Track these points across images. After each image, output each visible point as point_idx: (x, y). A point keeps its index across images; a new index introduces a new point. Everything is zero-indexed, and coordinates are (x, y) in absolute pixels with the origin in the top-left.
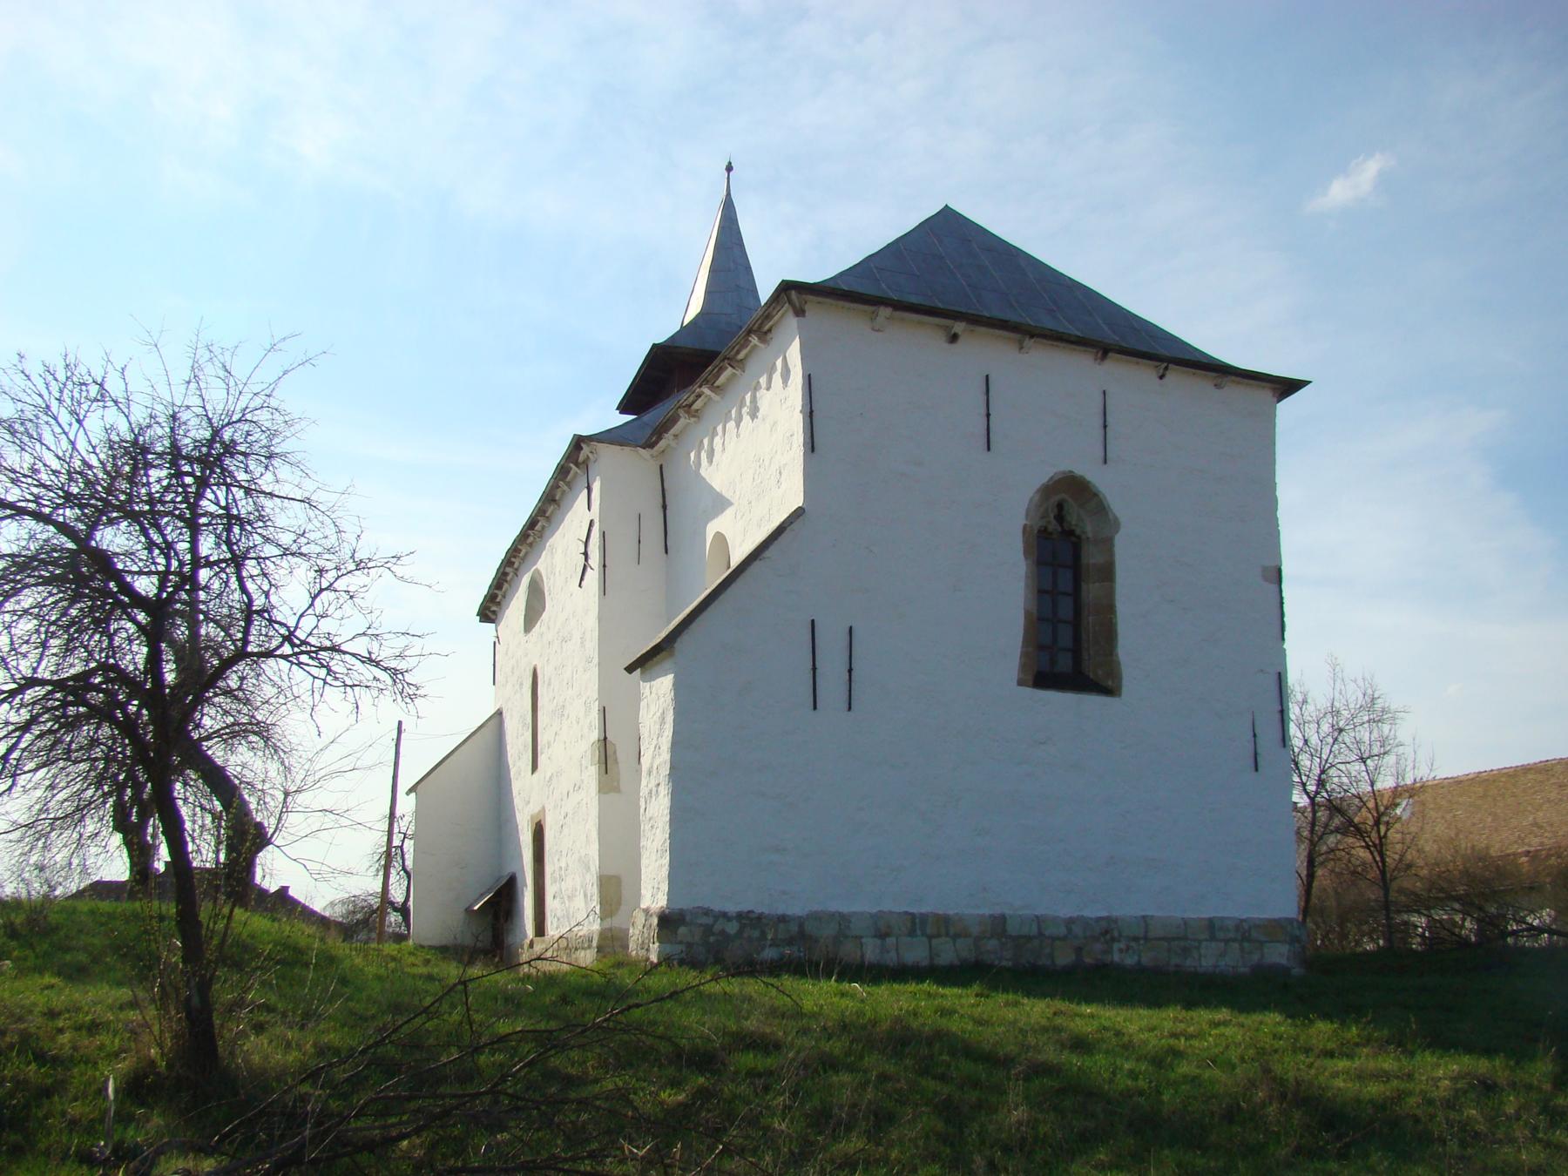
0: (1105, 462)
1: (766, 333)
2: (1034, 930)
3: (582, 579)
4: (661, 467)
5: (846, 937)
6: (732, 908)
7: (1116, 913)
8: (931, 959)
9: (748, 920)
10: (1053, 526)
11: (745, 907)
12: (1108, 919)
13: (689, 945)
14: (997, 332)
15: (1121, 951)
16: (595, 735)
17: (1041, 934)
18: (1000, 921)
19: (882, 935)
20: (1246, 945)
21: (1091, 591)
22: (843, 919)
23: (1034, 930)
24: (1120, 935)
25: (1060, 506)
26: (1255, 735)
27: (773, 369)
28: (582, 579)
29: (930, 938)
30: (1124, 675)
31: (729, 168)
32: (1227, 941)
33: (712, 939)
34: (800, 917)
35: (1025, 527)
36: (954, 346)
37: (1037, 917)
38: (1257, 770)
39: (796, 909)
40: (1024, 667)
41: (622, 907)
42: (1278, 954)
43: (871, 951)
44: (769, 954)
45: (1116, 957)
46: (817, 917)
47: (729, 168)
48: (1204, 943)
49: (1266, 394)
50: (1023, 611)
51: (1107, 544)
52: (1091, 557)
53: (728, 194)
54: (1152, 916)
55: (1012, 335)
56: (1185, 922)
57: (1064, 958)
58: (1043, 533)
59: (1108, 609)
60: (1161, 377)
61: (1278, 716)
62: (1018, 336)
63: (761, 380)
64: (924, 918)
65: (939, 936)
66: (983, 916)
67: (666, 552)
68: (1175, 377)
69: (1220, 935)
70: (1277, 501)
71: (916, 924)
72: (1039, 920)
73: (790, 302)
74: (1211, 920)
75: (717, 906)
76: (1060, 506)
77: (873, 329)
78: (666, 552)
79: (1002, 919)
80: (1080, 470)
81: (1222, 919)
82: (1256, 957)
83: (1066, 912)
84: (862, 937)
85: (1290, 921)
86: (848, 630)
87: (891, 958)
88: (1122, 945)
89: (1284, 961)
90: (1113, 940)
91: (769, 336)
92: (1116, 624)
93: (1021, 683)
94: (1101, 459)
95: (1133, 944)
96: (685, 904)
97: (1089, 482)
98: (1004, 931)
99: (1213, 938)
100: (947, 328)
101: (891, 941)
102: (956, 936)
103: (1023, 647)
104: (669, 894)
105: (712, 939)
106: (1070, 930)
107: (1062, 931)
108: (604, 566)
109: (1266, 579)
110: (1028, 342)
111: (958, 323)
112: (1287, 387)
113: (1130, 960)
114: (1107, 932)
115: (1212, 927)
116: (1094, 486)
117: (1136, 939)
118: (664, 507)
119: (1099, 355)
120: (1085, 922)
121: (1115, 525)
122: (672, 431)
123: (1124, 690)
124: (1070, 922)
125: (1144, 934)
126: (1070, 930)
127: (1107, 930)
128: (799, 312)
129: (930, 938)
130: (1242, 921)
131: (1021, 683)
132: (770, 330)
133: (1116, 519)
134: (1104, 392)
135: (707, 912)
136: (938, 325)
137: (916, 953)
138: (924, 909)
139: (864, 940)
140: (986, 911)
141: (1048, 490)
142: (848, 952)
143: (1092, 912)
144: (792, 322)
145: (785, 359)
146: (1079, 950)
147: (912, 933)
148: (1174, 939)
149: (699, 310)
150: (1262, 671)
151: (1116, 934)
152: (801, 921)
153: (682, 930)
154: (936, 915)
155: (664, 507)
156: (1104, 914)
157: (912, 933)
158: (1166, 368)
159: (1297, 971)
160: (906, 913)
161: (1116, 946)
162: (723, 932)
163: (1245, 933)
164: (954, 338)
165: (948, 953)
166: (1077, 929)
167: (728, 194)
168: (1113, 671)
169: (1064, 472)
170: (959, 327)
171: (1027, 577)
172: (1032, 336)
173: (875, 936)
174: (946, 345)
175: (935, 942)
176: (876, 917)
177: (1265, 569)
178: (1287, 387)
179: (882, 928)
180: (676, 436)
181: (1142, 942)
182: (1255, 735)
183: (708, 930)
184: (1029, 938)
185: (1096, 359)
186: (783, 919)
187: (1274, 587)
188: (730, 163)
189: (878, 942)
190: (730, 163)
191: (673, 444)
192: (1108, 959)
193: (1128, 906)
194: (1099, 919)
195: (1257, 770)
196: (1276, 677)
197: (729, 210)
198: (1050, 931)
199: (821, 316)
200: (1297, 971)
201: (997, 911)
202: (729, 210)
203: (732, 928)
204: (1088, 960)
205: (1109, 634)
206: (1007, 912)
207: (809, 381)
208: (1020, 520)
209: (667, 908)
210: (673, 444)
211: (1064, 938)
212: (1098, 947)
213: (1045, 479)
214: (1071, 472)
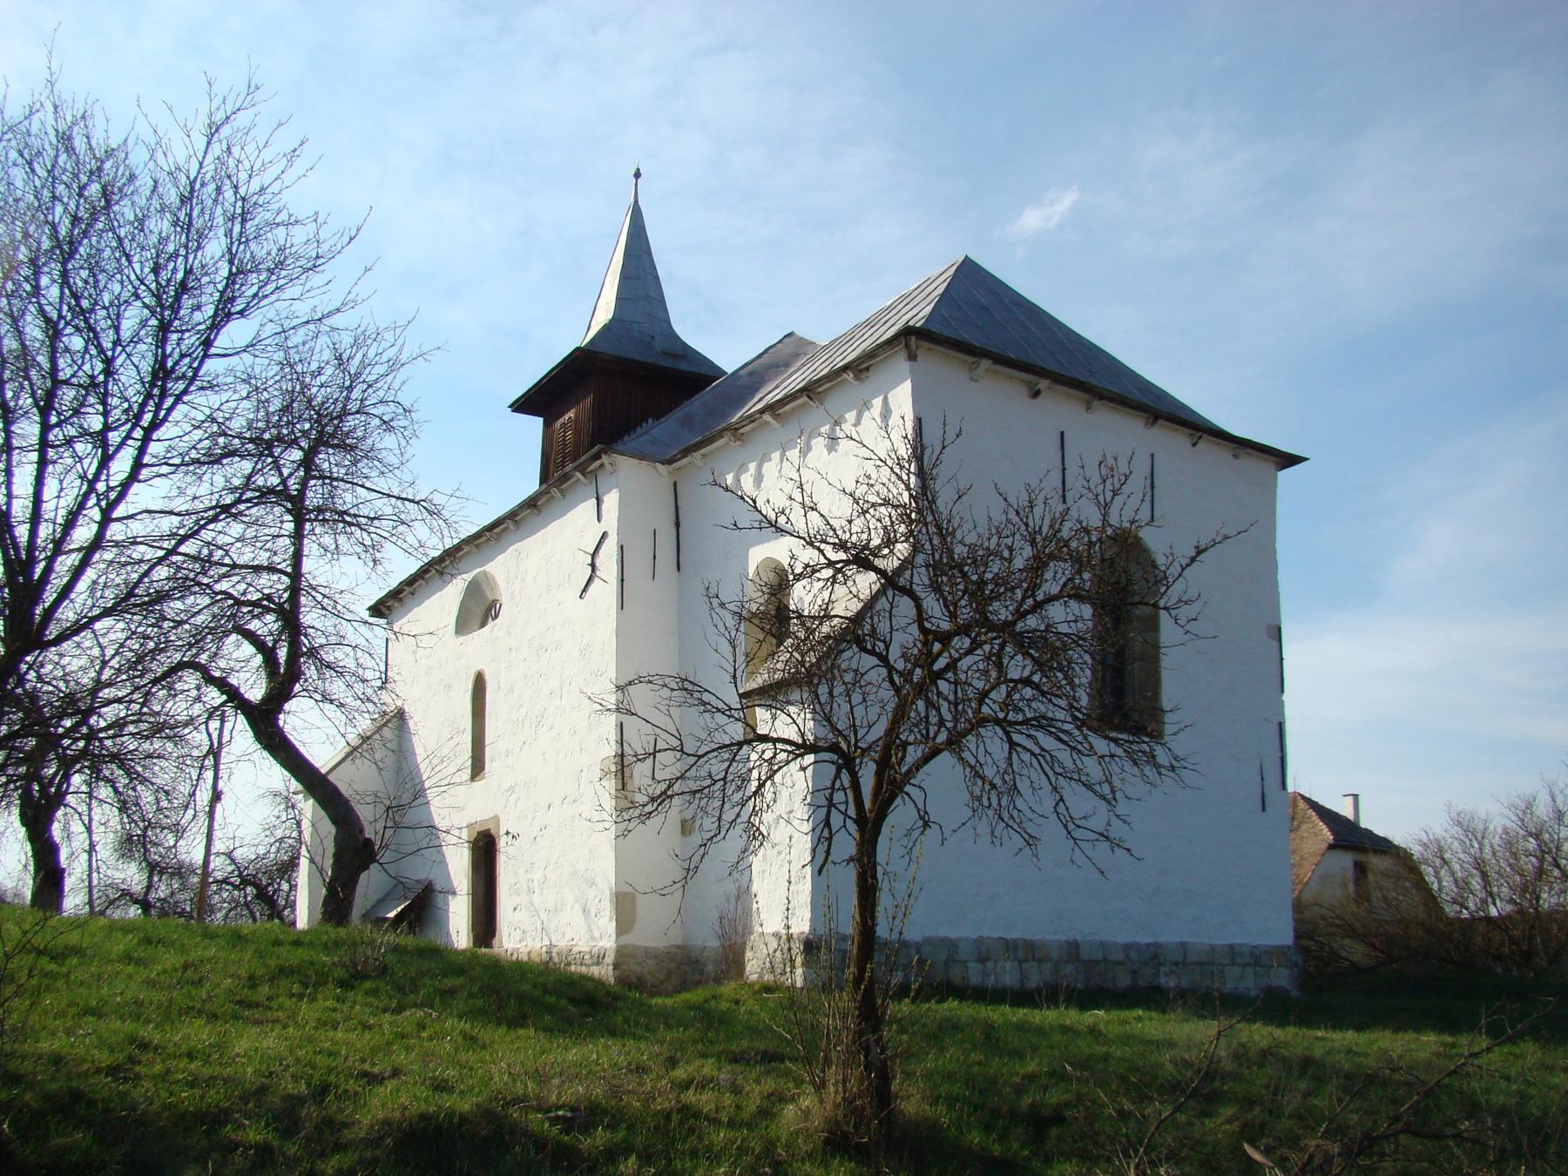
1: (861, 371)
2: (1100, 956)
3: (585, 590)
4: (675, 484)
5: (955, 961)
7: (1159, 940)
8: (1022, 982)
12: (1156, 945)
14: (1071, 391)
16: (611, 750)
17: (1105, 959)
19: (983, 960)
20: (1257, 969)
22: (951, 945)
27: (866, 406)
28: (585, 590)
29: (1021, 962)
31: (638, 175)
32: (1244, 965)
34: (917, 943)
36: (1037, 401)
38: (1264, 810)
41: (637, 925)
42: (1281, 978)
46: (929, 941)
47: (638, 175)
48: (1227, 968)
49: (1266, 466)
53: (636, 201)
55: (1076, 393)
56: (1213, 948)
57: (1124, 981)
60: (1194, 445)
61: (1279, 761)
62: (1086, 396)
63: (847, 416)
64: (1015, 942)
65: (1027, 961)
66: (1059, 941)
67: (679, 569)
69: (1239, 960)
71: (1010, 947)
73: (907, 346)
74: (1231, 947)
77: (971, 379)
78: (679, 569)
81: (1240, 945)
83: (1123, 937)
84: (966, 962)
85: (1289, 947)
89: (1284, 984)
90: (1160, 964)
91: (865, 373)
95: (1174, 967)
96: (821, 931)
98: (1078, 955)
99: (1233, 963)
100: (1029, 384)
101: (990, 964)
102: (1040, 961)
104: (812, 920)
106: (1127, 956)
107: (1121, 956)
108: (622, 580)
110: (1097, 404)
112: (1289, 460)
114: (1155, 956)
117: (1176, 964)
118: (678, 525)
119: (1151, 420)
122: (703, 451)
124: (1127, 947)
125: (1183, 958)
126: (1127, 956)
127: (1154, 955)
128: (912, 357)
130: (1255, 947)
132: (867, 369)
134: (1152, 455)
136: (1023, 381)
139: (968, 965)
142: (956, 975)
143: (1144, 938)
144: (901, 364)
145: (886, 399)
146: (1134, 973)
149: (610, 316)
151: (1162, 959)
154: (1024, 940)
155: (678, 525)
156: (1151, 940)
158: (1200, 437)
159: (1295, 993)
160: (1000, 938)
161: (1163, 969)
163: (1258, 958)
164: (1036, 394)
166: (1133, 955)
167: (636, 201)
170: (1043, 384)
172: (1101, 398)
173: (978, 961)
174: (1028, 400)
175: (1025, 965)
176: (979, 941)
177: (1269, 627)
178: (1289, 460)
180: (704, 456)
184: (1096, 962)
185: (1146, 424)
188: (638, 170)
189: (980, 965)
190: (638, 170)
191: (699, 463)
193: (1169, 934)
194: (1148, 945)
195: (1264, 810)
196: (1277, 727)
198: (1113, 956)
200: (1295, 993)
204: (1141, 983)
206: (1079, 938)
209: (810, 933)
210: (699, 463)
211: (1121, 963)
212: (1148, 971)
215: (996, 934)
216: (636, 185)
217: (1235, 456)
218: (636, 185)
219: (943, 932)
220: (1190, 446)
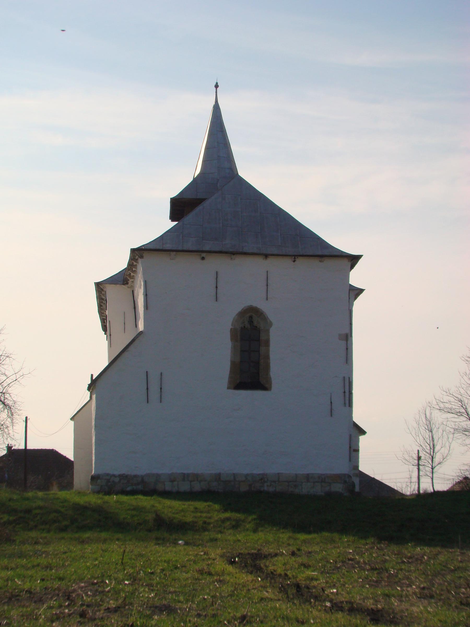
0: (267, 300)
6: (117, 473)
9: (122, 477)
10: (248, 326)
11: (122, 472)
12: (263, 474)
15: (268, 486)
18: (218, 477)
19: (172, 481)
21: (263, 349)
22: (158, 475)
24: (268, 480)
25: (251, 317)
26: (331, 403)
30: (273, 382)
31: (217, 86)
33: (109, 484)
35: (231, 329)
36: (204, 261)
37: (234, 474)
40: (230, 382)
43: (168, 487)
44: (129, 489)
45: (266, 488)
46: (148, 475)
47: (217, 86)
51: (268, 331)
52: (263, 337)
54: (282, 473)
56: (296, 475)
59: (267, 357)
60: (294, 261)
64: (188, 475)
68: (300, 261)
70: (353, 305)
71: (185, 477)
72: (234, 475)
74: (308, 475)
75: (111, 472)
76: (251, 317)
77: (171, 259)
79: (220, 474)
80: (254, 305)
81: (313, 474)
83: (246, 471)
86: (160, 374)
87: (175, 489)
89: (340, 490)
92: (269, 363)
93: (228, 388)
94: (265, 298)
96: (100, 472)
97: (259, 309)
99: (308, 481)
101: (175, 483)
103: (229, 374)
105: (109, 484)
109: (340, 339)
110: (233, 256)
111: (203, 254)
113: (271, 489)
114: (261, 479)
115: (308, 477)
116: (261, 310)
121: (271, 324)
124: (247, 475)
127: (263, 478)
129: (191, 482)
130: (322, 474)
131: (228, 388)
133: (271, 322)
135: (108, 475)
137: (185, 487)
138: (190, 472)
139: (166, 483)
142: (160, 487)
147: (184, 480)
148: (291, 482)
150: (336, 376)
151: (266, 479)
152: (142, 477)
153: (99, 481)
157: (184, 480)
161: (266, 484)
162: (113, 481)
164: (203, 258)
165: (197, 487)
168: (269, 380)
169: (248, 306)
170: (204, 255)
171: (231, 348)
179: (172, 478)
181: (277, 483)
182: (331, 403)
183: (108, 481)
186: (136, 476)
187: (344, 343)
188: (217, 83)
190: (217, 83)
192: (262, 489)
194: (259, 475)
197: (217, 110)
199: (149, 259)
202: (217, 110)
203: (117, 480)
207: (145, 282)
208: (229, 326)
213: (239, 309)
214: (252, 305)
215: (179, 471)
216: (216, 92)
218: (216, 92)
219: (155, 471)
220: (293, 263)
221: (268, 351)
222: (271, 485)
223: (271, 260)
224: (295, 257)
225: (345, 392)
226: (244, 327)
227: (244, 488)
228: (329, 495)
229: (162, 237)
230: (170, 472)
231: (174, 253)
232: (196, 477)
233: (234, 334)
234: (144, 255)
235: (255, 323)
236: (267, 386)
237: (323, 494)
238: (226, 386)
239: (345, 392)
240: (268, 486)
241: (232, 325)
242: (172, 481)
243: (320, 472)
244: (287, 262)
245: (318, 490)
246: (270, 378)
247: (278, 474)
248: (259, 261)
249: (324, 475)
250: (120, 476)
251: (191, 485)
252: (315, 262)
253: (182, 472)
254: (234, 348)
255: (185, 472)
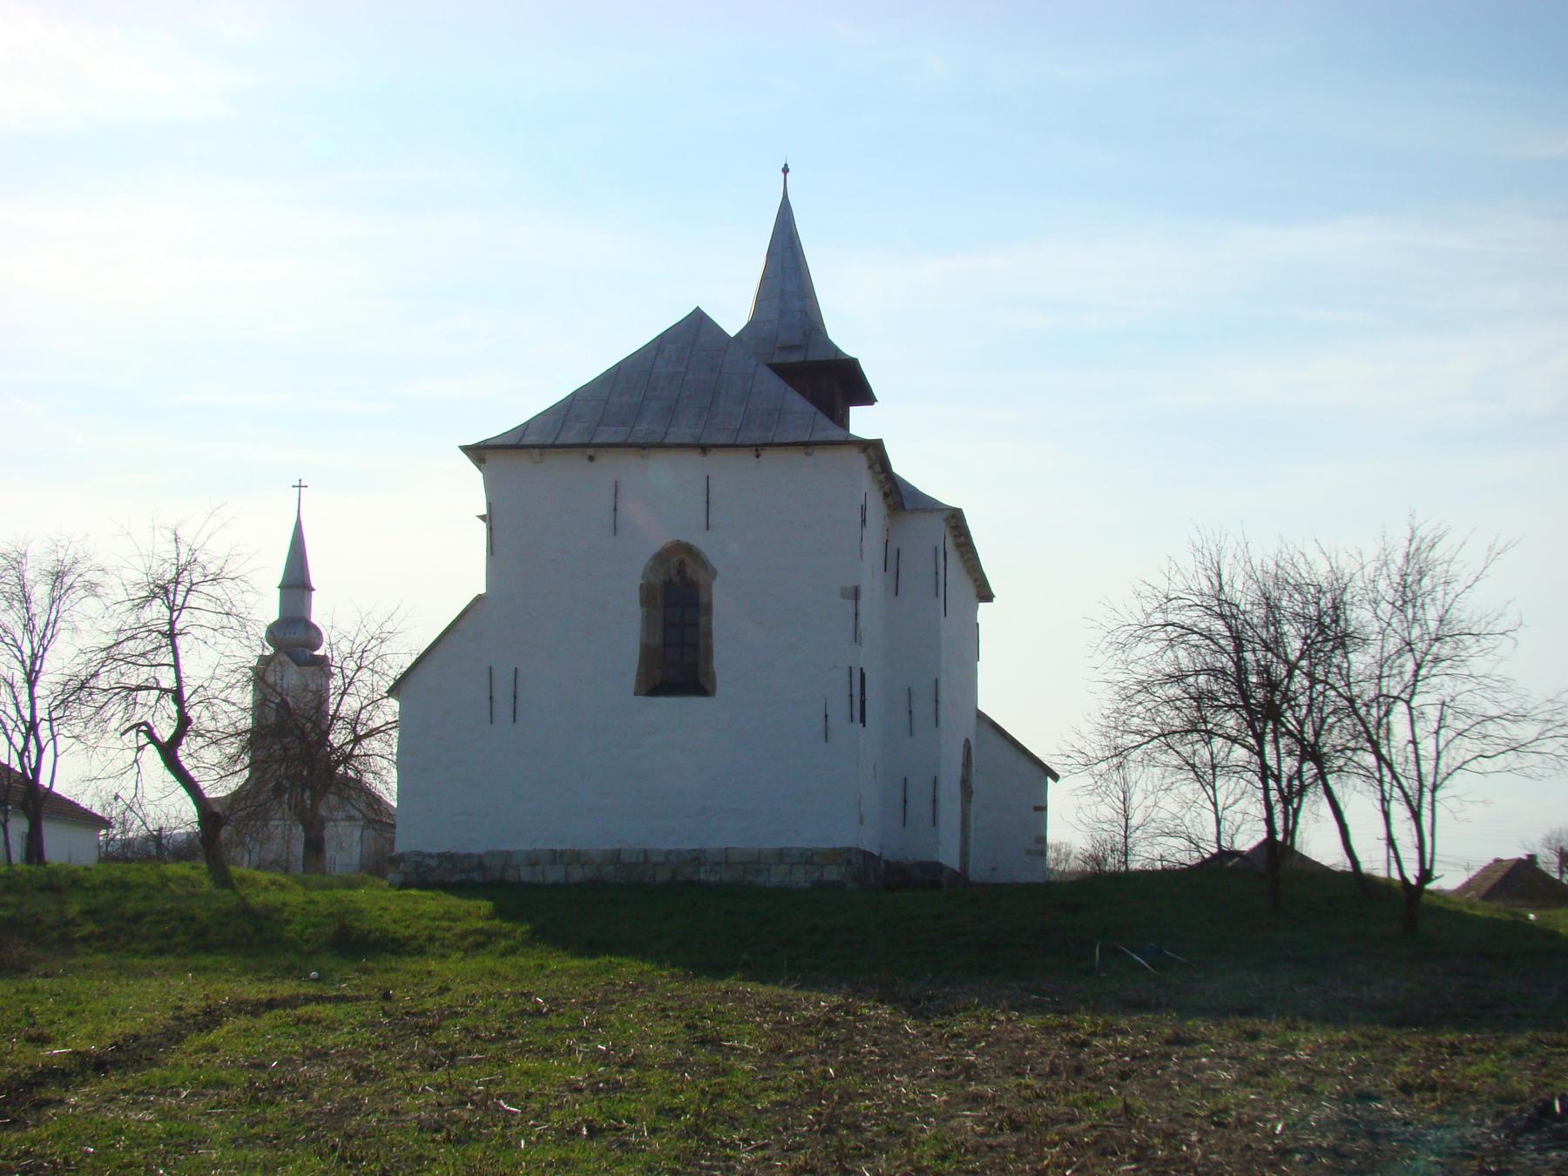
2: (641, 859)
6: (435, 850)
9: (446, 858)
13: (406, 874)
15: (706, 872)
18: (615, 856)
21: (703, 620)
22: (508, 854)
23: (641, 859)
25: (682, 563)
26: (826, 716)
30: (718, 678)
31: (786, 170)
32: (792, 865)
34: (480, 855)
35: (642, 585)
37: (645, 851)
39: (476, 849)
40: (639, 683)
45: (702, 876)
46: (492, 854)
47: (786, 170)
50: (638, 648)
51: (710, 587)
52: (703, 599)
54: (734, 848)
58: (668, 584)
59: (709, 635)
60: (758, 456)
64: (562, 853)
68: (767, 455)
71: (556, 857)
76: (682, 563)
79: (619, 852)
82: (816, 876)
84: (518, 866)
88: (708, 868)
93: (636, 694)
101: (540, 867)
105: (421, 870)
109: (843, 596)
113: (713, 878)
114: (695, 859)
115: (781, 855)
117: (719, 864)
120: (679, 852)
121: (713, 574)
123: (718, 692)
127: (697, 858)
130: (807, 850)
131: (636, 694)
133: (714, 569)
135: (418, 853)
138: (564, 847)
140: (608, 847)
141: (662, 557)
143: (687, 846)
151: (703, 860)
152: (480, 857)
153: (402, 865)
170: (591, 452)
182: (826, 716)
183: (419, 864)
186: (468, 856)
187: (850, 604)
188: (786, 165)
190: (786, 165)
192: (696, 878)
194: (690, 851)
195: (826, 740)
201: (617, 846)
203: (434, 863)
204: (679, 878)
205: (709, 652)
208: (638, 581)
217: (807, 454)
219: (503, 847)
221: (709, 622)
222: (711, 872)
223: (715, 457)
224: (758, 448)
225: (851, 695)
226: (671, 581)
227: (663, 876)
228: (820, 885)
229: (527, 425)
230: (530, 849)
231: (537, 451)
232: (577, 857)
233: (648, 595)
234: (486, 457)
235: (689, 572)
236: (708, 687)
237: (808, 885)
238: (632, 691)
239: (851, 695)
240: (706, 872)
241: (643, 577)
242: (534, 864)
243: (806, 845)
244: (746, 457)
245: (800, 878)
246: (714, 673)
247: (726, 849)
248: (692, 459)
249: (811, 850)
250: (440, 856)
251: (566, 872)
252: (797, 456)
253: (549, 847)
254: (648, 620)
255: (558, 847)
